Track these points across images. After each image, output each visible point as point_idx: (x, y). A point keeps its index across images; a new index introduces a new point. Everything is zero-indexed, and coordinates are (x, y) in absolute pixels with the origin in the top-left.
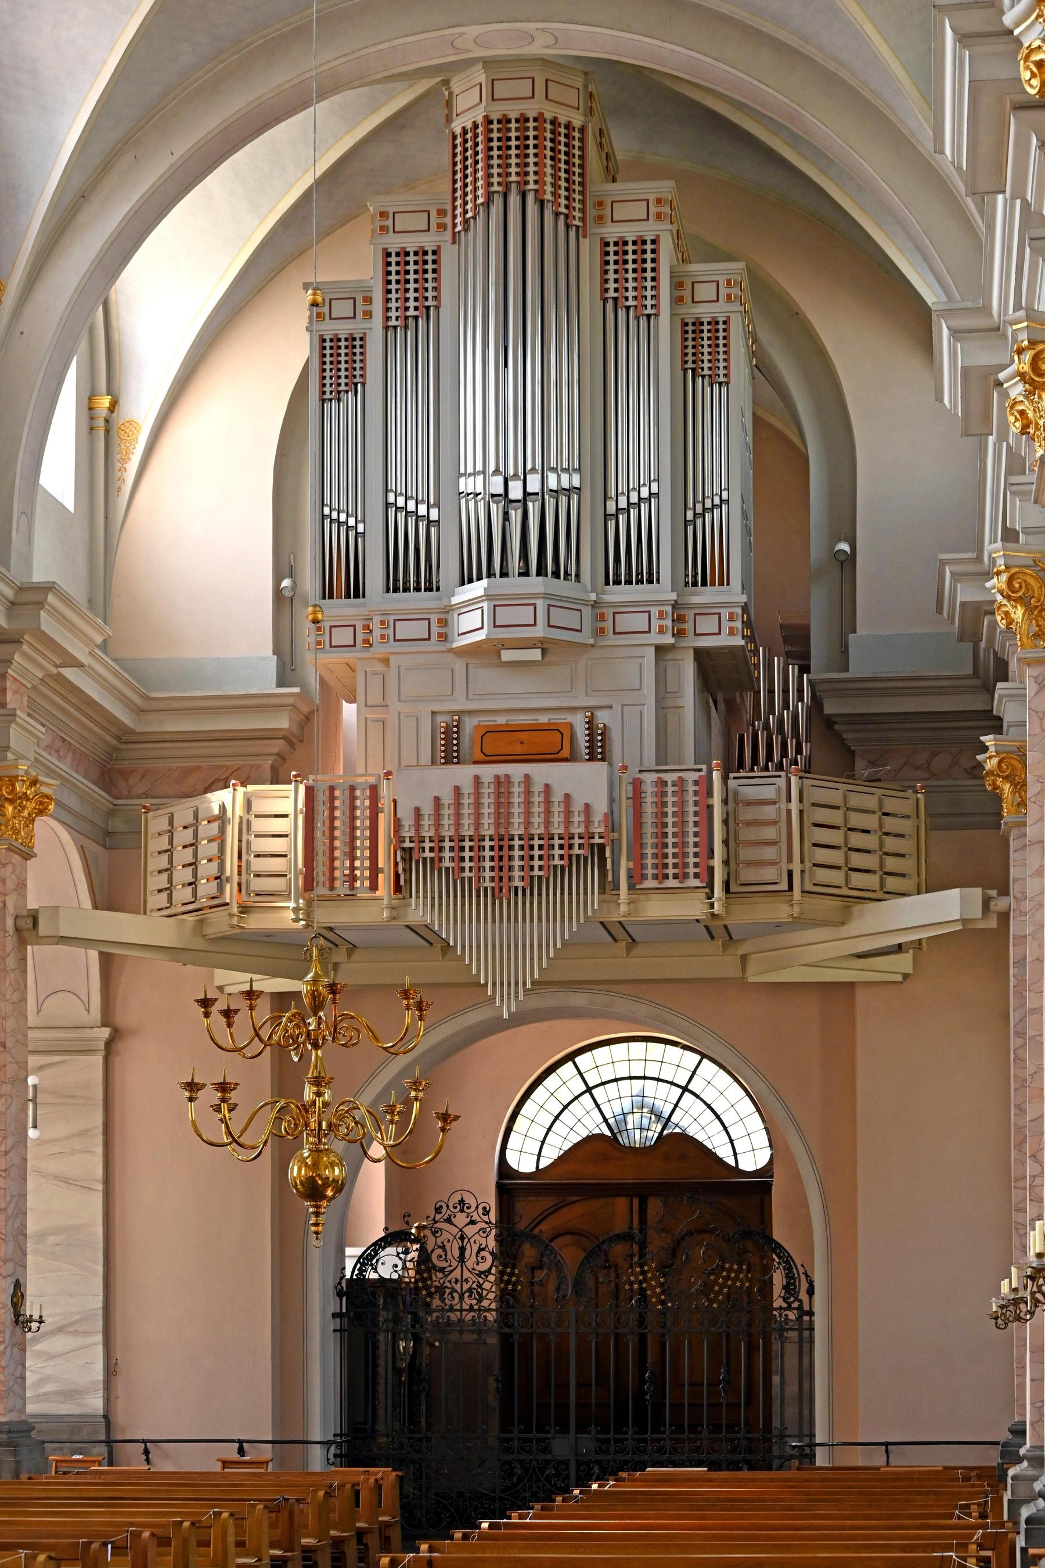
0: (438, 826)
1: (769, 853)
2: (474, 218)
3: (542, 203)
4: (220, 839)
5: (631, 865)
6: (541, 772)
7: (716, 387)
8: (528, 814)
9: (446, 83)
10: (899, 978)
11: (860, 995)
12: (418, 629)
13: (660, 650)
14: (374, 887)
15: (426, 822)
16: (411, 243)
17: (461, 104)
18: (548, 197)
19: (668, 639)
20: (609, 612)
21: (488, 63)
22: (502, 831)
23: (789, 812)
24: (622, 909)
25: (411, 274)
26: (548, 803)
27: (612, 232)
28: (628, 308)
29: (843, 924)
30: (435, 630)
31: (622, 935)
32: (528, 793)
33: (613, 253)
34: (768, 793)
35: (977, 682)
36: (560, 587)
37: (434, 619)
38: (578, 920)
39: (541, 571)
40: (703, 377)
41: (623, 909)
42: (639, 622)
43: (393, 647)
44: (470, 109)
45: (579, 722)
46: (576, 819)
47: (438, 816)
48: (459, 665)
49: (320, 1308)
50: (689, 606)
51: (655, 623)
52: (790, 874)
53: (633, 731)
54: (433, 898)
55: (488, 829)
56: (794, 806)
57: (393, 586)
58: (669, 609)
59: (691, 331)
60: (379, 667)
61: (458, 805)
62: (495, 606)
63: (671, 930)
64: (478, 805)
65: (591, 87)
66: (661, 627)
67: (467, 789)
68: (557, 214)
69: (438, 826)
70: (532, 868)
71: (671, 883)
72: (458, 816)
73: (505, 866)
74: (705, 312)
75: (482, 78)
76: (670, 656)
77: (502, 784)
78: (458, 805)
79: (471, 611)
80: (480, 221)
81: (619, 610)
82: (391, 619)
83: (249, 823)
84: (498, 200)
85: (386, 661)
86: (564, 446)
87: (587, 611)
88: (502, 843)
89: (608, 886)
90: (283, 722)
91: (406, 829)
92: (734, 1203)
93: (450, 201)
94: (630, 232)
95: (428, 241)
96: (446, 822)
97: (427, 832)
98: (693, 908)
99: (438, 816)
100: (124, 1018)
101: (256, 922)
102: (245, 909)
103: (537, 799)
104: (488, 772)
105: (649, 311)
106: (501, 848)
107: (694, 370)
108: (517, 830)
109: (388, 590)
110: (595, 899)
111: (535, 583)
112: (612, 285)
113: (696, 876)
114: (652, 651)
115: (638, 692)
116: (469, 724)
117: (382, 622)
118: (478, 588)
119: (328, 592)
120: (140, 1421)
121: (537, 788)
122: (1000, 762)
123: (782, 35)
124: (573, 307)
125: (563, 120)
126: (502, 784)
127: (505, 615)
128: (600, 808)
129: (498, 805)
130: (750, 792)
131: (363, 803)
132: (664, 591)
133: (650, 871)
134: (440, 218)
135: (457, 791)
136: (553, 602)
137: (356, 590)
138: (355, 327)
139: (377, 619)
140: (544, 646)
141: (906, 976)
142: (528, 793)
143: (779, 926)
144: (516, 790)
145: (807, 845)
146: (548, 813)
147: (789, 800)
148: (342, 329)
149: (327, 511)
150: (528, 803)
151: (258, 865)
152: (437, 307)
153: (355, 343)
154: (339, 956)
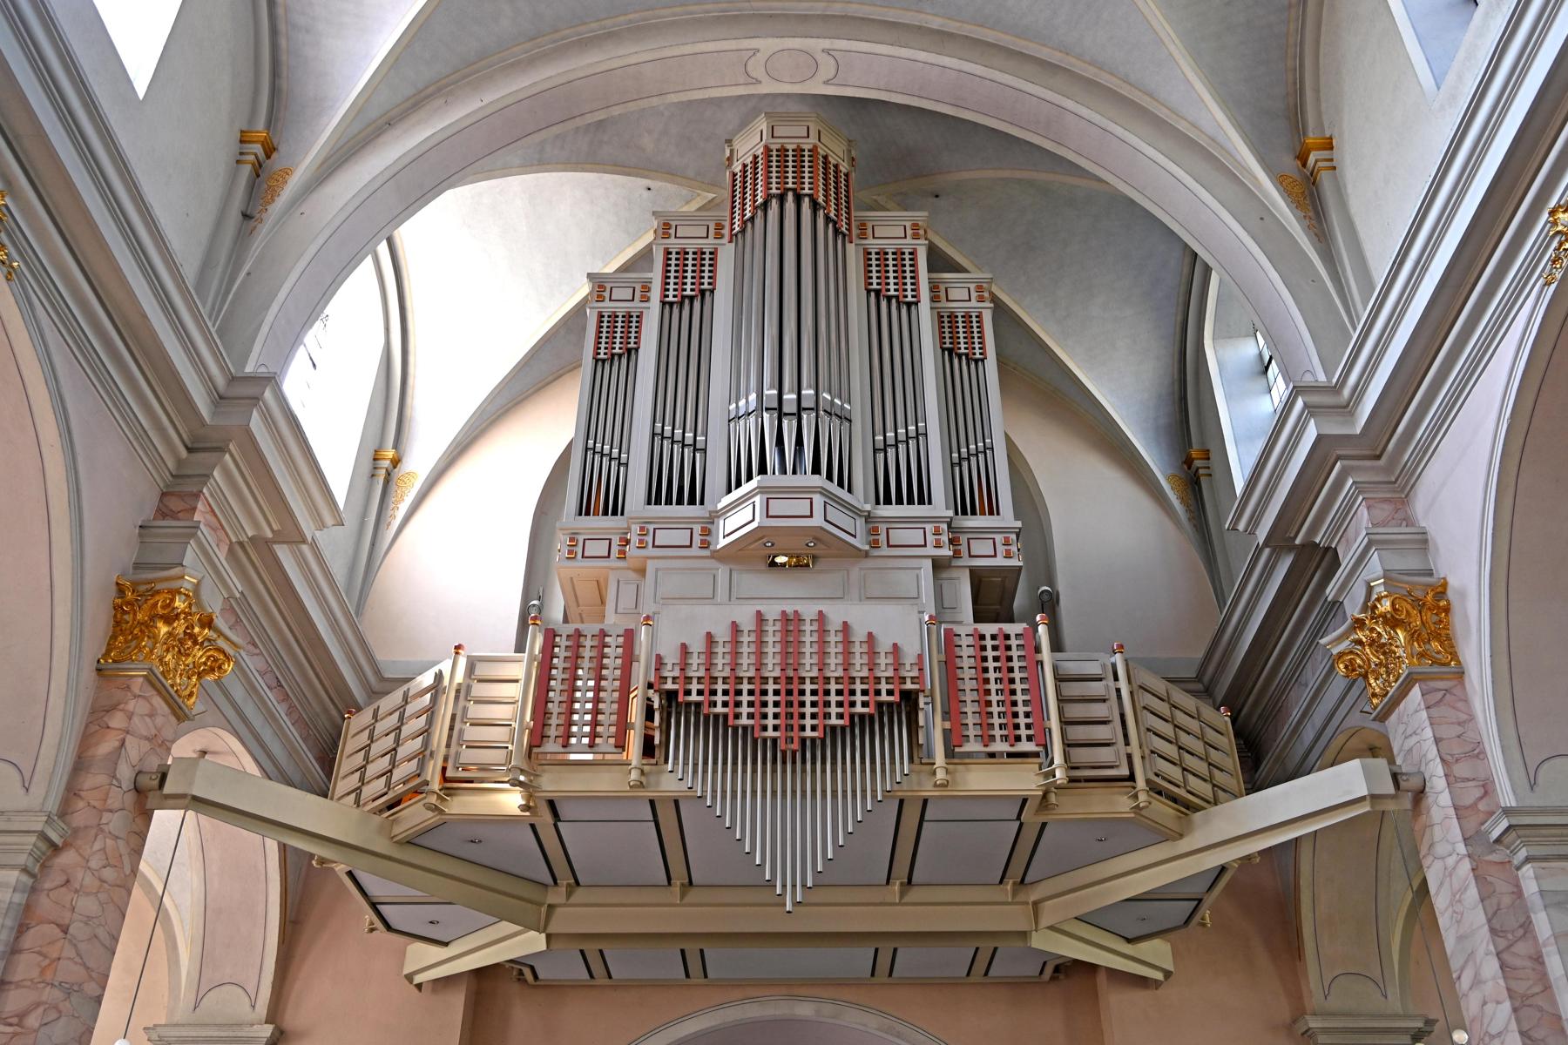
0: (709, 667)
1: (1101, 733)
2: (752, 219)
4: (431, 711)
5: (948, 725)
7: (973, 366)
8: (823, 654)
9: (729, 142)
10: (1159, 976)
12: (681, 537)
14: (621, 746)
15: (694, 661)
18: (821, 200)
19: (947, 552)
20: (882, 528)
22: (790, 673)
23: (1118, 690)
26: (847, 642)
27: (873, 244)
29: (1181, 836)
30: (697, 539)
32: (823, 631)
33: (875, 261)
34: (1093, 669)
35: (1200, 687)
37: (697, 529)
38: (874, 796)
39: (816, 470)
40: (960, 356)
41: (940, 775)
42: (915, 536)
43: (650, 551)
46: (883, 660)
47: (710, 653)
48: (722, 572)
50: (963, 530)
51: (931, 539)
52: (1129, 757)
54: (695, 765)
55: (772, 669)
56: (1123, 684)
57: (654, 498)
58: (945, 526)
59: (946, 322)
60: (632, 575)
61: (735, 642)
64: (761, 643)
65: (853, 154)
66: (938, 541)
67: (747, 623)
68: (827, 218)
69: (709, 667)
70: (827, 716)
71: (1000, 746)
72: (736, 654)
74: (959, 308)
75: (764, 127)
76: (944, 575)
78: (735, 642)
80: (759, 221)
82: (651, 527)
83: (469, 688)
84: (774, 203)
85: (642, 572)
87: (860, 522)
88: (790, 688)
91: (669, 667)
95: (707, 244)
96: (719, 661)
97: (696, 670)
98: (1025, 780)
99: (710, 653)
101: (463, 805)
102: (450, 785)
103: (832, 638)
105: (909, 299)
106: (789, 692)
107: (950, 351)
108: (809, 669)
109: (649, 503)
112: (875, 281)
113: (1029, 738)
114: (929, 563)
117: (642, 529)
119: (585, 509)
121: (834, 624)
122: (1393, 605)
123: (1044, 53)
127: (777, 507)
129: (785, 643)
131: (613, 652)
132: (940, 505)
133: (972, 732)
135: (735, 629)
139: (636, 528)
141: (1168, 974)
142: (823, 631)
144: (807, 627)
145: (1142, 729)
146: (847, 653)
147: (1116, 679)
148: (621, 308)
149: (591, 442)
150: (822, 643)
151: (472, 733)
152: (712, 291)
153: (632, 322)
154: (556, 896)
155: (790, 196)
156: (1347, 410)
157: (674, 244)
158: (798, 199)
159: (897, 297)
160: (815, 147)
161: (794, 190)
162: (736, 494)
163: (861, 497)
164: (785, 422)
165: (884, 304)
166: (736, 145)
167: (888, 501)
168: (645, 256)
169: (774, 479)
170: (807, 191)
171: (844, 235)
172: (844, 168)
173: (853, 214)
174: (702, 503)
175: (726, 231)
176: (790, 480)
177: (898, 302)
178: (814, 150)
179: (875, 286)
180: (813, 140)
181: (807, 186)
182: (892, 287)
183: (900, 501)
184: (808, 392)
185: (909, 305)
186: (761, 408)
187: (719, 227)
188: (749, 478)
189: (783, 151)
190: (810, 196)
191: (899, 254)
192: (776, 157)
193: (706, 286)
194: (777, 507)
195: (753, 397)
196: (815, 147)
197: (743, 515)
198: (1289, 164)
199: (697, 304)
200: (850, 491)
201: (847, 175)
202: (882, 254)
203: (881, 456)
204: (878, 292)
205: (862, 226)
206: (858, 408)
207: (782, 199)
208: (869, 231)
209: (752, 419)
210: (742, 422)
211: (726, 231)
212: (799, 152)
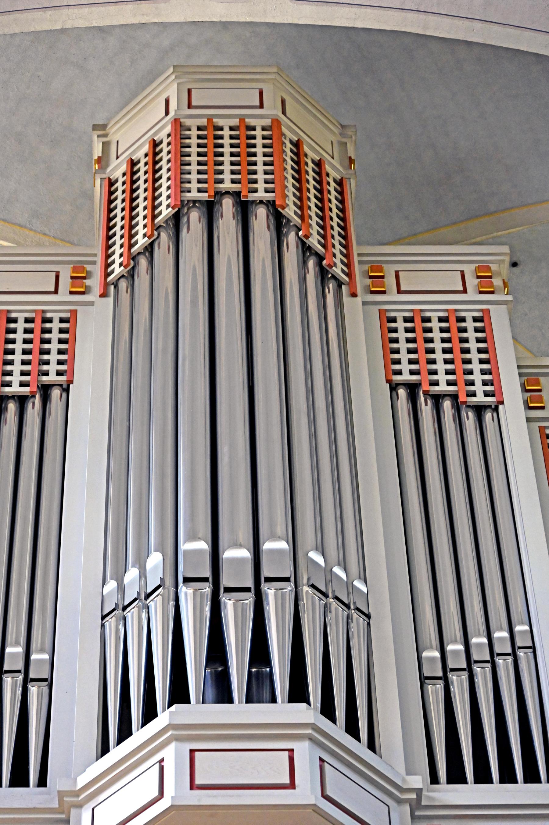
2: (150, 249)
3: (279, 222)
27: (399, 305)
28: (437, 399)
62: (192, 751)
65: (351, 153)
68: (305, 249)
75: (172, 93)
84: (195, 219)
93: (99, 259)
95: (56, 306)
105: (480, 399)
125: (311, 153)
155: (228, 203)
158: (244, 209)
159: (454, 397)
160: (276, 123)
161: (237, 194)
162: (117, 752)
164: (229, 605)
165: (426, 410)
166: (115, 134)
167: (456, 776)
169: (199, 711)
170: (261, 195)
171: (340, 284)
172: (334, 170)
173: (356, 250)
174: (42, 782)
175: (95, 282)
176: (239, 712)
177: (457, 408)
178: (274, 129)
179: (406, 377)
180: (272, 109)
181: (261, 186)
182: (442, 378)
183: (483, 776)
184: (275, 545)
185: (479, 410)
186: (176, 578)
187: (79, 277)
188: (150, 713)
189: (211, 132)
190: (270, 204)
191: (453, 322)
193: (52, 378)
194: (210, 769)
195: (155, 560)
196: (276, 123)
197: (140, 787)
199: (33, 412)
200: (372, 746)
201: (340, 183)
202: (418, 322)
203: (435, 691)
204: (412, 389)
205: (376, 277)
206: (383, 586)
207: (210, 209)
208: (390, 281)
209: (156, 604)
210: (132, 614)
211: (95, 282)
212: (244, 132)
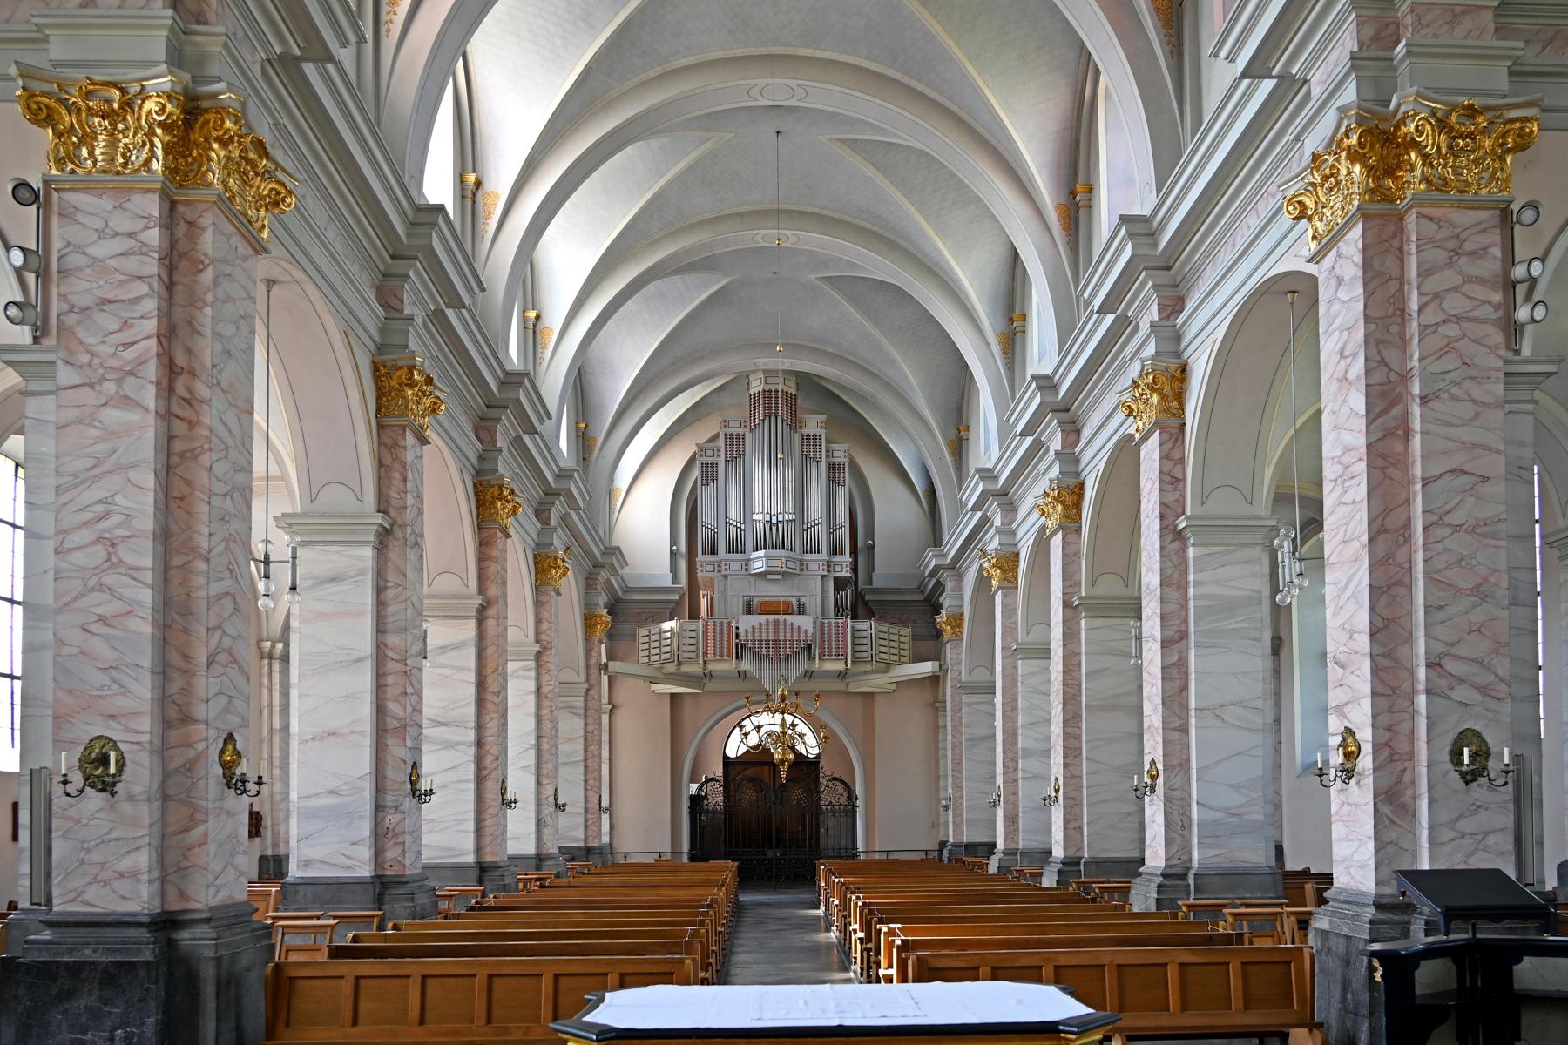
6: (790, 618)
11: (877, 698)
12: (737, 567)
13: (823, 577)
16: (735, 431)
17: (753, 384)
21: (764, 371)
24: (817, 665)
25: (735, 443)
27: (805, 432)
31: (809, 675)
33: (806, 439)
36: (791, 554)
42: (815, 567)
44: (757, 386)
45: (794, 601)
49: (686, 804)
53: (813, 602)
57: (728, 551)
63: (828, 674)
73: (774, 650)
74: (837, 461)
77: (776, 622)
79: (758, 561)
81: (808, 562)
86: (790, 505)
89: (812, 658)
90: (676, 597)
92: (805, 768)
94: (811, 432)
95: (741, 431)
98: (840, 666)
100: (618, 700)
104: (763, 618)
110: (807, 662)
111: (783, 553)
115: (815, 592)
116: (756, 600)
118: (761, 553)
120: (623, 845)
124: (793, 455)
126: (776, 622)
127: (771, 563)
128: (810, 631)
130: (859, 627)
132: (824, 556)
134: (744, 423)
136: (788, 559)
137: (714, 552)
138: (714, 460)
140: (784, 574)
143: (865, 673)
148: (710, 460)
153: (714, 466)
156: (945, 556)
157: (729, 431)
163: (797, 554)
168: (716, 436)
192: (769, 396)
198: (953, 434)
